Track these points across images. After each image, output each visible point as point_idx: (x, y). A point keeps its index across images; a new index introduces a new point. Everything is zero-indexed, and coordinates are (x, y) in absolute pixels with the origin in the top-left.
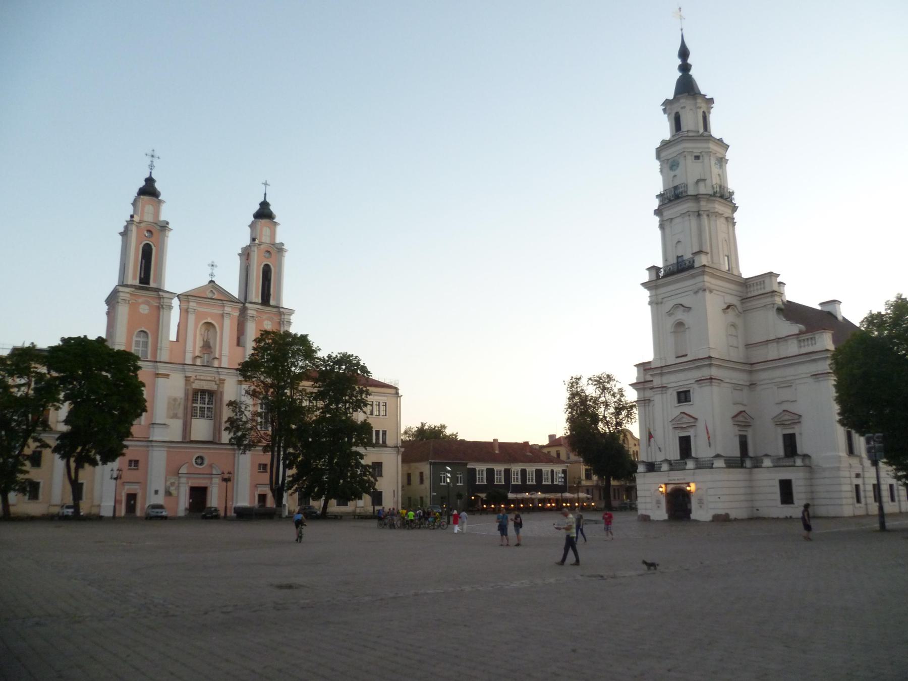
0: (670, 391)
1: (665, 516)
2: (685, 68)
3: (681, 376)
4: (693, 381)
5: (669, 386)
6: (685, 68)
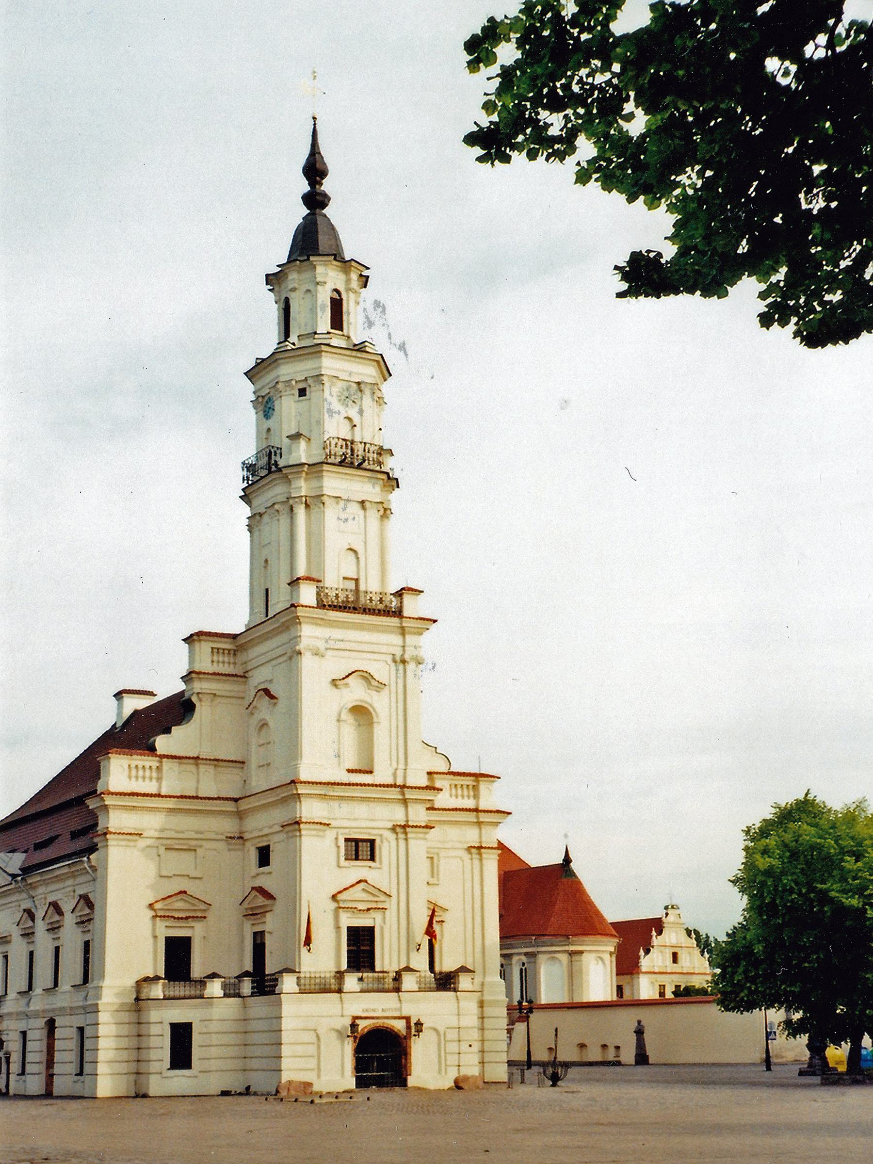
0: (330, 834)
1: (351, 1083)
2: (315, 201)
3: (361, 810)
4: (390, 825)
5: (334, 823)
6: (315, 201)
